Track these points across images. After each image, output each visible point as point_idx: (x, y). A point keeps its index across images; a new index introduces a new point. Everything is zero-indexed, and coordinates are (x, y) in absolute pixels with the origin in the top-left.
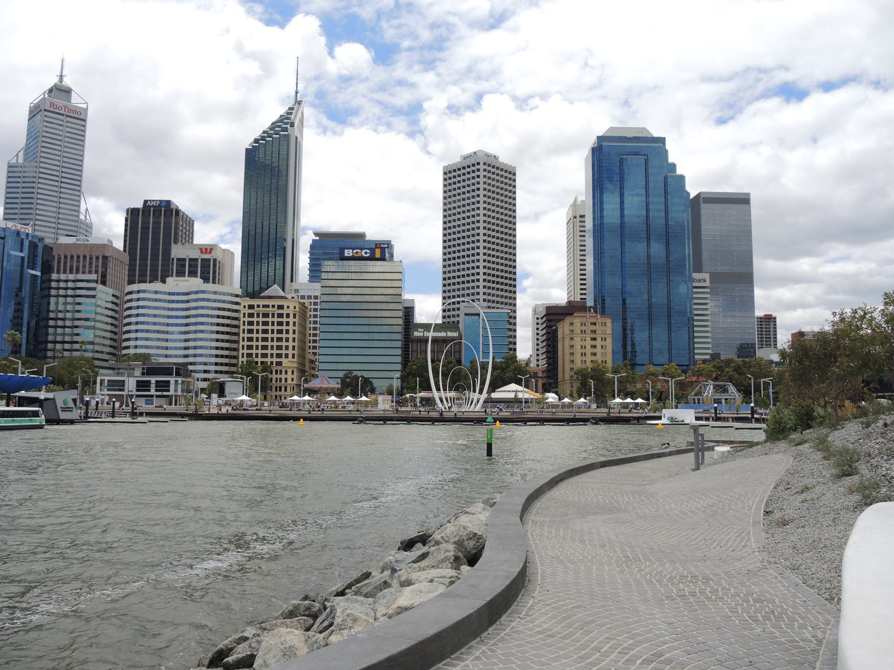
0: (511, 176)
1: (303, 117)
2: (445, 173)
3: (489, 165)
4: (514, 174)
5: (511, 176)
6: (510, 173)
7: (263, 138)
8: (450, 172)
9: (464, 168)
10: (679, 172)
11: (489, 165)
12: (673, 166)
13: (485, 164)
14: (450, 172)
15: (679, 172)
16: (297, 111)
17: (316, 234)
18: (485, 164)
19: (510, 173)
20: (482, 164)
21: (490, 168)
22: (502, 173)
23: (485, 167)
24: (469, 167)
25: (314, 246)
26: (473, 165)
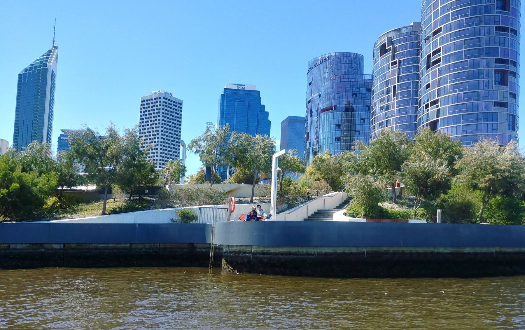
0: (179, 105)
1: (57, 57)
2: (142, 102)
3: (166, 99)
4: (181, 104)
5: (179, 105)
6: (179, 104)
7: (31, 69)
8: (144, 101)
9: (152, 100)
10: (266, 110)
11: (166, 99)
12: (263, 106)
13: (164, 98)
14: (144, 101)
15: (266, 110)
16: (53, 53)
17: (63, 131)
18: (164, 98)
19: (179, 104)
20: (162, 98)
21: (167, 101)
22: (174, 104)
23: (164, 100)
24: (155, 99)
25: (61, 140)
26: (157, 98)
